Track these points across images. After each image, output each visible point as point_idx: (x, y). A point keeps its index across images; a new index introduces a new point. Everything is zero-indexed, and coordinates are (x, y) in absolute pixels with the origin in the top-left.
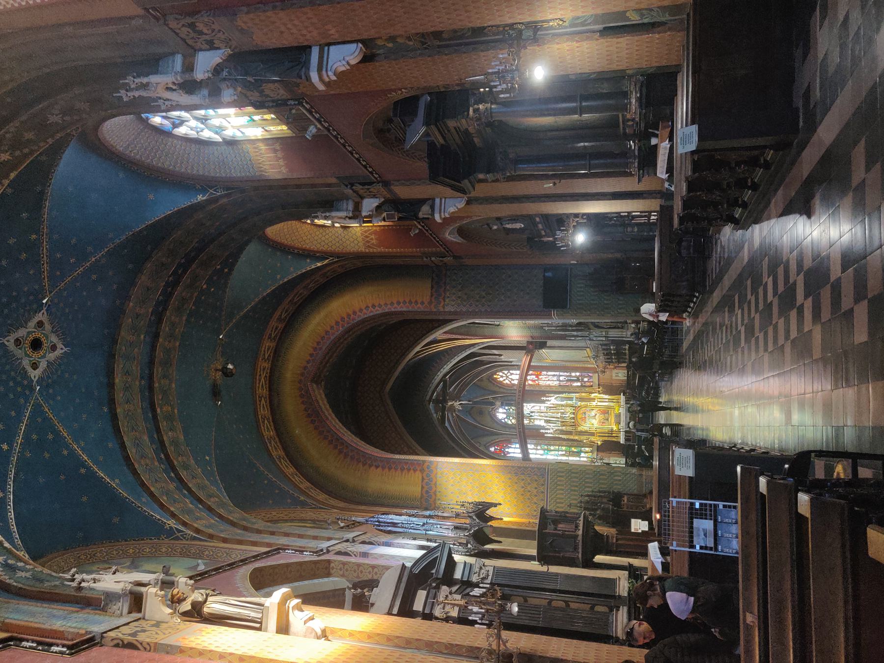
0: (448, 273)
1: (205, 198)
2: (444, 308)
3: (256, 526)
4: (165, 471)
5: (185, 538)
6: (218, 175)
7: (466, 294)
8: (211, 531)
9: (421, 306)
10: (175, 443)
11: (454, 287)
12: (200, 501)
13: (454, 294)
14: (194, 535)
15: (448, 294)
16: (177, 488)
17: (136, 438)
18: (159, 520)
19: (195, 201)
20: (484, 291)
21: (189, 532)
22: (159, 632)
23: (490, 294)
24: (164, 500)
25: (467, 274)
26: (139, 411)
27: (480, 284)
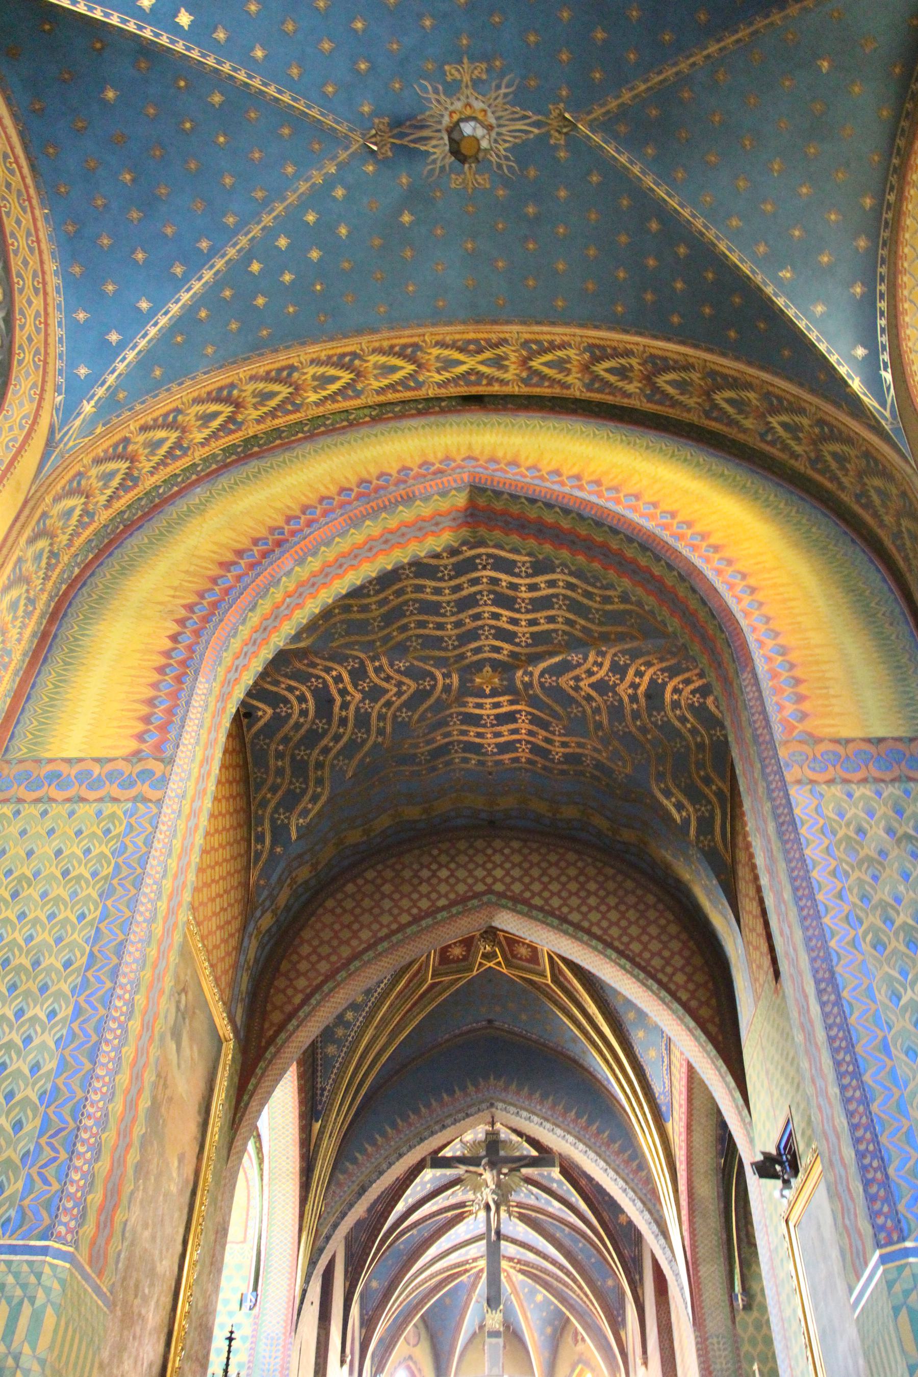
2: (799, 782)
7: (883, 853)
11: (900, 812)
13: (871, 814)
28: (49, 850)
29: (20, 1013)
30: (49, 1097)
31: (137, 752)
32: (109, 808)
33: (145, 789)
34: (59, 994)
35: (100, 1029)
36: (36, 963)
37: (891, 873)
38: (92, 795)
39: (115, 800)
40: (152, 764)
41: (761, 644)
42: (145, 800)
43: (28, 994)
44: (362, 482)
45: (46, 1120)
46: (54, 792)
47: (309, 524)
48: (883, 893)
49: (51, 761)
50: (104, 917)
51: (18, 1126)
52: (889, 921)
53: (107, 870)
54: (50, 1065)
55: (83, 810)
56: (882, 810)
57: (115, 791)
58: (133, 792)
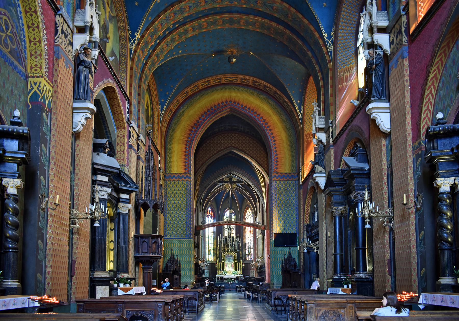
0: (294, 182)
1: (325, 38)
2: (274, 180)
3: (142, 84)
4: (169, 28)
5: (131, 45)
6: (338, 46)
7: (282, 192)
8: (136, 59)
9: (275, 167)
10: (186, 32)
12: (154, 50)
13: (282, 186)
14: (133, 50)
15: (282, 182)
16: (160, 36)
17: (185, 9)
18: (139, 29)
19: (323, 33)
20: (284, 202)
21: (134, 46)
22: (66, 45)
23: (282, 205)
24: (151, 30)
25: (293, 192)
26: (201, 9)
27: (288, 200)
28: (177, 189)
29: (180, 213)
30: (186, 223)
32: (184, 182)
33: (188, 179)
34: (184, 210)
35: (190, 214)
36: (180, 206)
37: (282, 195)
38: (181, 180)
39: (184, 181)
40: (188, 175)
41: (274, 153)
42: (188, 181)
43: (180, 210)
45: (187, 225)
46: (175, 179)
47: (203, 120)
49: (173, 173)
50: (187, 199)
51: (184, 226)
52: (280, 202)
54: (185, 219)
55: (180, 182)
56: (284, 185)
57: (184, 179)
58: (186, 180)
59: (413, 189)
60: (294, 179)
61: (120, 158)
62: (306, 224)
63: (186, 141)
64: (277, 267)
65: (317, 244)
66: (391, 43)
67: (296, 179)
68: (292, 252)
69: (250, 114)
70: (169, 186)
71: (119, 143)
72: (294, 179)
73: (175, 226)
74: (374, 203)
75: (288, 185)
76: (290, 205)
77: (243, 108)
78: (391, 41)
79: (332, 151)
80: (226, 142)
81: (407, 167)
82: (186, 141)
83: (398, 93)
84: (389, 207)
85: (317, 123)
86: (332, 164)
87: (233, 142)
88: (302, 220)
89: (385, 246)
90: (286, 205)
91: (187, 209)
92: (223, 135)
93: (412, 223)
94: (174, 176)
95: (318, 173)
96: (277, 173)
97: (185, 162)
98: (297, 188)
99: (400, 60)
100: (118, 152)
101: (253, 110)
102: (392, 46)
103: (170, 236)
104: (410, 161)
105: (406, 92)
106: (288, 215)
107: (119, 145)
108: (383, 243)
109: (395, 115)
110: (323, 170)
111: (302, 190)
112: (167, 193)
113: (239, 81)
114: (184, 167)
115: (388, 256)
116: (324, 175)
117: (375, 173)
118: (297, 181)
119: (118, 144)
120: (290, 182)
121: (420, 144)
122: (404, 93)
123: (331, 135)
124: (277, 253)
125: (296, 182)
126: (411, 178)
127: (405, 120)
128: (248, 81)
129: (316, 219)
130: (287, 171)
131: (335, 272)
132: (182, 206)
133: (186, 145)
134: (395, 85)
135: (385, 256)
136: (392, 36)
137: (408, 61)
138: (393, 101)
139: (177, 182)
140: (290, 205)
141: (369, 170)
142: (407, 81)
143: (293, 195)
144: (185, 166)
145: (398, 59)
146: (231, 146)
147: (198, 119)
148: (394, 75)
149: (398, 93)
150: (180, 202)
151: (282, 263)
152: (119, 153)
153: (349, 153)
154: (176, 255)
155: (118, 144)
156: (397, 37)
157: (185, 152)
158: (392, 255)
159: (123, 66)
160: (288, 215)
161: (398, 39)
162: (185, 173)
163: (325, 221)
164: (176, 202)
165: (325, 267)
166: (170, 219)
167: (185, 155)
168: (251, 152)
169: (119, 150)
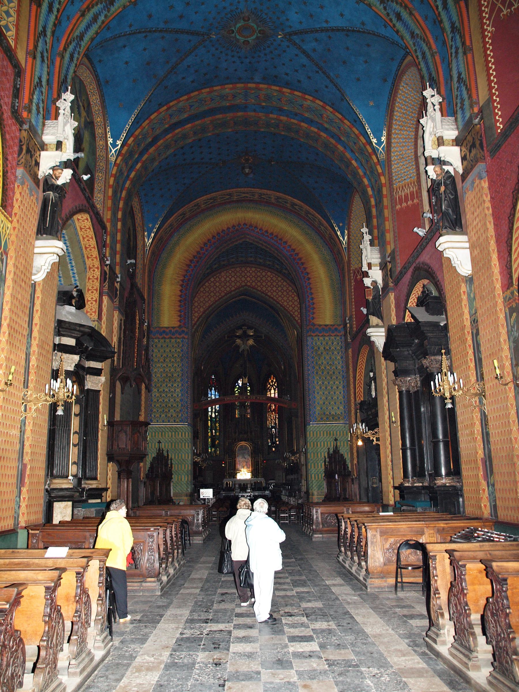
0: (338, 338)
20: (325, 368)
23: (323, 373)
28: (168, 350)
30: (181, 400)
31: (180, 325)
32: (178, 340)
37: (322, 358)
40: (184, 329)
44: (218, 233)
47: (207, 250)
48: (320, 363)
53: (181, 355)
54: (180, 395)
55: (173, 340)
57: (178, 336)
59: (509, 356)
60: (338, 334)
61: (91, 309)
62: (358, 401)
63: (182, 281)
64: (318, 467)
65: (376, 432)
66: (464, 159)
67: (341, 334)
68: (338, 444)
69: (273, 241)
70: (156, 346)
71: (90, 288)
72: (338, 334)
73: (164, 405)
74: (455, 374)
75: (330, 343)
76: (334, 373)
77: (263, 234)
78: (463, 156)
79: (392, 296)
80: (238, 279)
81: (498, 325)
82: (182, 281)
83: (477, 224)
84: (477, 380)
85: (369, 256)
86: (393, 314)
87: (249, 279)
88: (353, 396)
89: (476, 438)
90: (328, 373)
91: (182, 380)
92: (233, 270)
93: (512, 405)
94: (164, 332)
95: (373, 327)
96: (314, 325)
97: (180, 311)
98: (343, 347)
99: (477, 181)
100: (88, 301)
101: (277, 236)
102: (465, 163)
103: (157, 421)
104: (502, 316)
105: (488, 223)
106: (332, 388)
107: (90, 292)
108: (472, 433)
109: (476, 252)
110: (381, 323)
111: (350, 350)
112: (154, 356)
113: (256, 197)
114: (179, 318)
115: (481, 453)
116: (383, 330)
117: (454, 331)
118: (343, 337)
119: (89, 290)
120: (333, 338)
121: (512, 293)
122: (485, 224)
123: (389, 273)
124: (317, 445)
125: (341, 338)
126: (505, 341)
127: (490, 261)
128: (269, 197)
129: (373, 394)
130: (328, 322)
131: (406, 476)
132: (175, 375)
133: (181, 286)
134: (473, 214)
135: (477, 453)
136: (464, 149)
137: (487, 184)
138: (472, 233)
139: (168, 340)
140: (334, 373)
141: (446, 326)
142: (488, 208)
143: (339, 357)
144: (180, 316)
145: (475, 179)
146: (246, 285)
147: (199, 250)
148: (470, 199)
149: (477, 224)
150: (172, 370)
151: (325, 462)
152: (89, 303)
153: (416, 300)
154: (165, 450)
155: (89, 290)
156: (470, 152)
157: (180, 296)
158: (486, 451)
159: (99, 184)
160: (332, 388)
161: (472, 155)
162: (180, 326)
163: (387, 398)
164: (167, 370)
165: (390, 468)
166: (157, 395)
167: (180, 301)
168: (275, 294)
169: (89, 299)
